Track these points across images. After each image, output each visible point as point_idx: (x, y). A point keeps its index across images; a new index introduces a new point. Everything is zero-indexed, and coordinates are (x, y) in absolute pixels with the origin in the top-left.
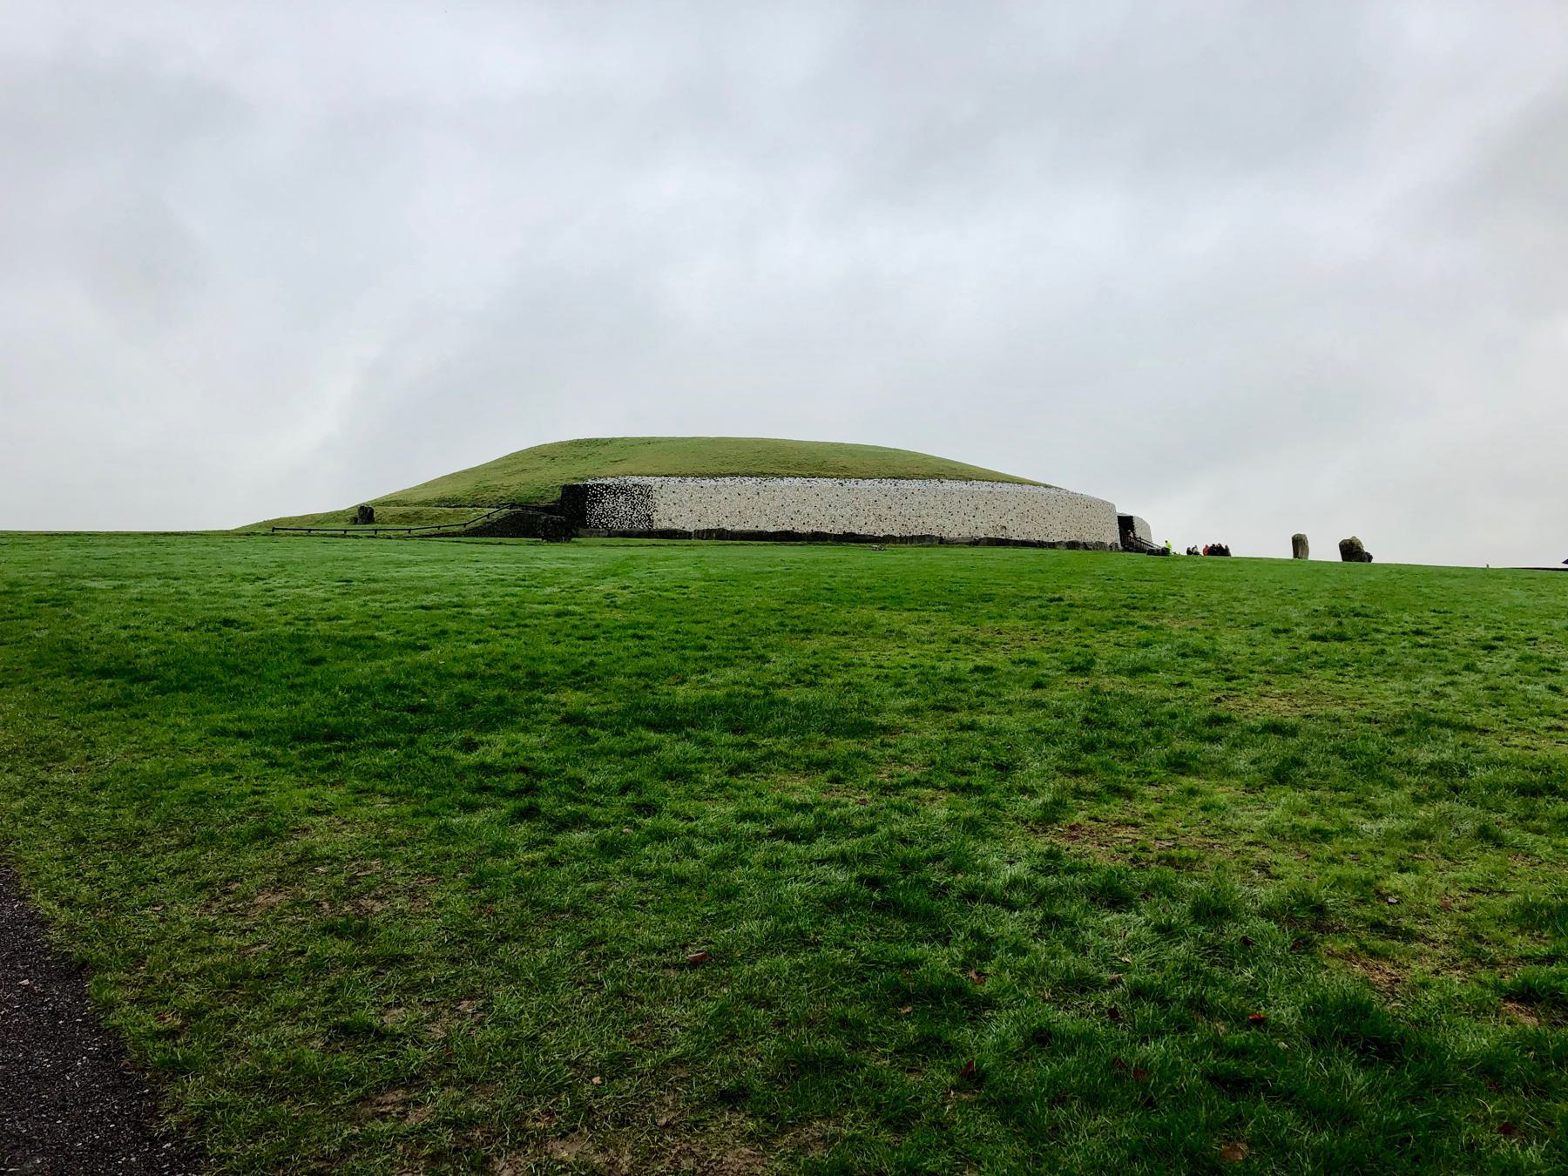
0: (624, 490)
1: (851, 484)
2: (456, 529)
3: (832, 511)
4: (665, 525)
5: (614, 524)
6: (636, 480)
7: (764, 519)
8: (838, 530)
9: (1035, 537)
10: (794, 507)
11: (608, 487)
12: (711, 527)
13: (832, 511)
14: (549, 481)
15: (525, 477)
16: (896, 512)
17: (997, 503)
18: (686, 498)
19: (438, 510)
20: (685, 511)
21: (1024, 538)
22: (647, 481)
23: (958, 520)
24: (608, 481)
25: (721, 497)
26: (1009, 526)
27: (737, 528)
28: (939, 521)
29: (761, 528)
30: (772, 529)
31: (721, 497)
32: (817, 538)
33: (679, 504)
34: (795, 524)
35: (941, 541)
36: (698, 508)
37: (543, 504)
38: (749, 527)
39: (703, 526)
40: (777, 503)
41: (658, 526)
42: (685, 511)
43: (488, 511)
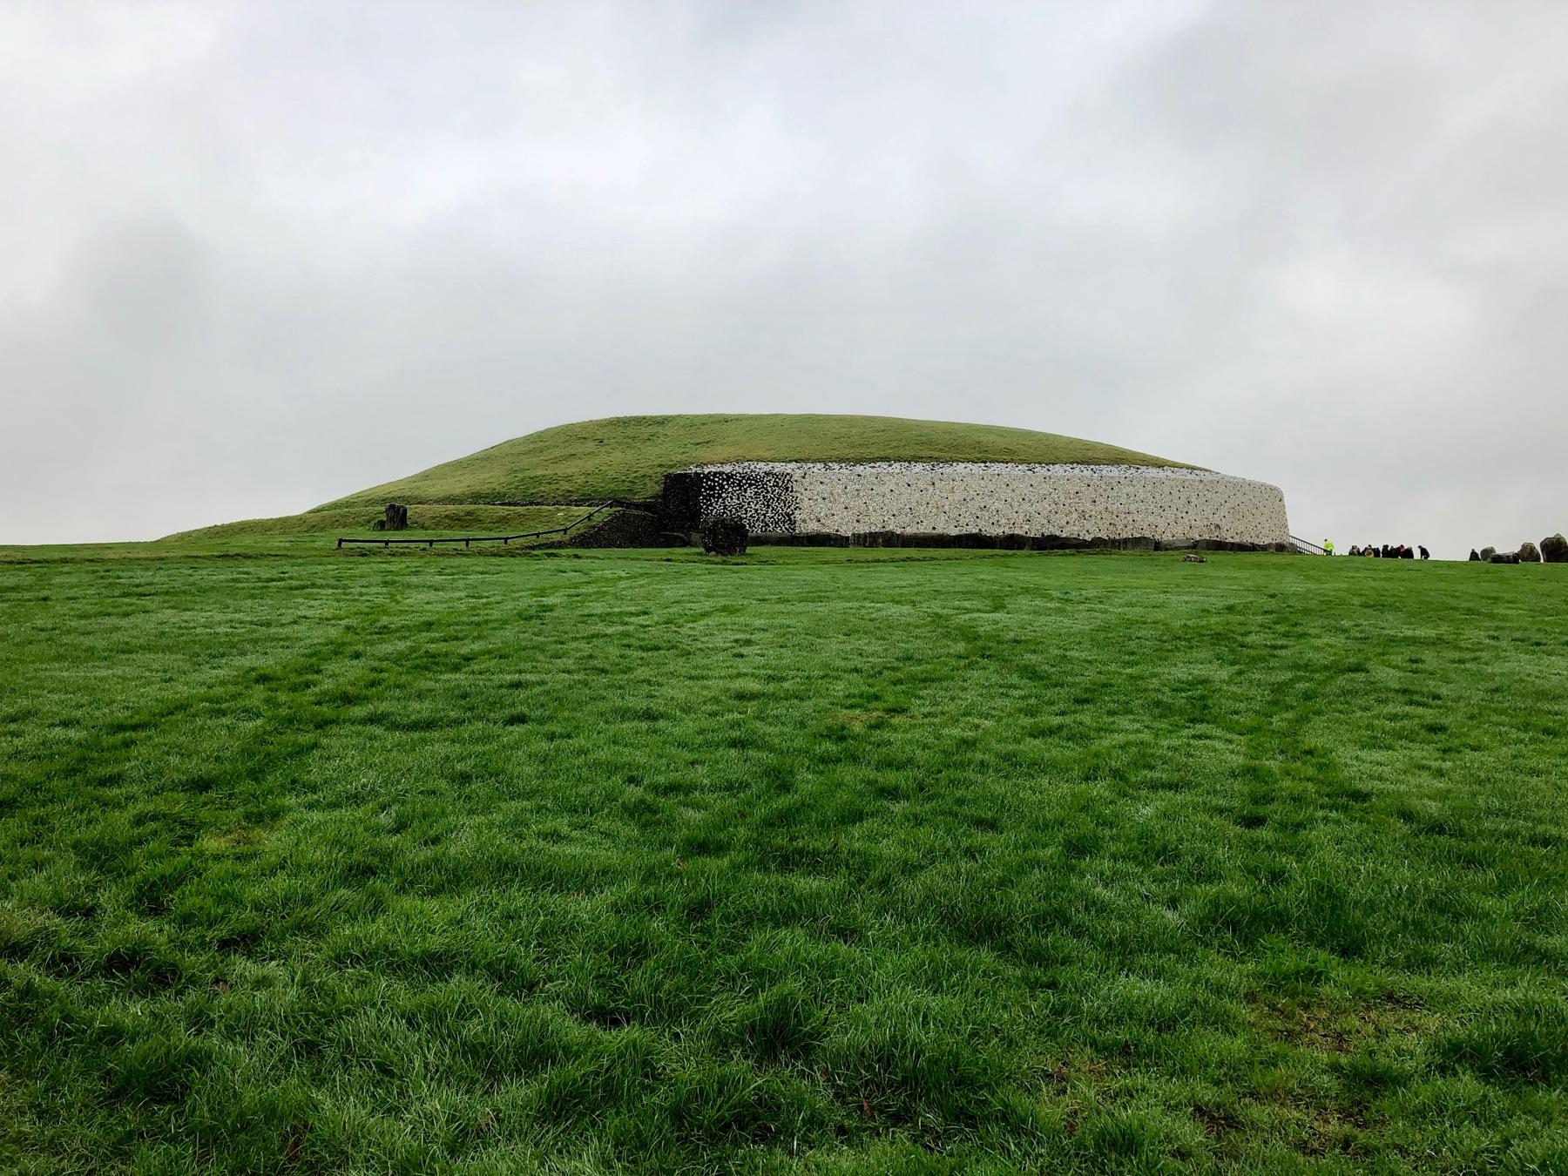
0: (751, 480)
2: (556, 537)
3: (1026, 506)
4: (812, 527)
7: (943, 518)
8: (1034, 530)
9: (1247, 540)
10: (979, 502)
11: (729, 477)
12: (874, 529)
13: (1026, 506)
14: (643, 468)
15: (590, 465)
16: (1101, 508)
17: (1209, 495)
18: (839, 489)
19: (501, 511)
20: (838, 508)
21: (1237, 540)
22: (779, 468)
23: (1171, 519)
24: (727, 469)
25: (885, 489)
26: (1223, 524)
27: (909, 531)
28: (1151, 519)
29: (939, 531)
30: (954, 532)
31: (885, 489)
32: (1013, 542)
33: (829, 500)
34: (981, 523)
35: (1158, 546)
36: (856, 505)
37: (637, 499)
38: (924, 529)
39: (863, 529)
40: (958, 496)
42: (838, 508)
43: (584, 511)
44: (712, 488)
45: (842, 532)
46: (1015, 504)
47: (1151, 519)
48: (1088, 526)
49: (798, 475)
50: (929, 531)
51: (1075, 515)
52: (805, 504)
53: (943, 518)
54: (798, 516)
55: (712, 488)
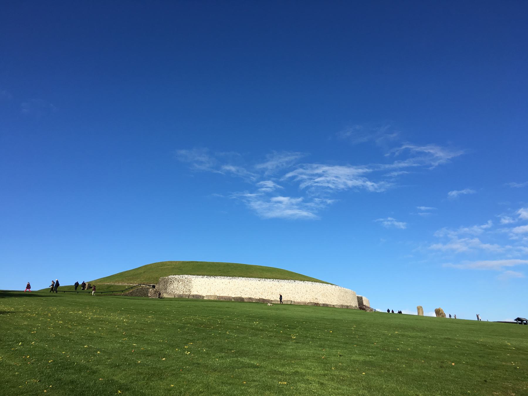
0: (182, 280)
1: (262, 280)
5: (177, 292)
6: (186, 276)
12: (212, 294)
13: (255, 290)
27: (221, 295)
28: (294, 295)
29: (230, 296)
30: (233, 296)
34: (242, 294)
39: (209, 294)
41: (192, 293)
45: (203, 295)
46: (252, 289)
47: (294, 295)
48: (274, 296)
49: (193, 279)
53: (231, 292)
54: (192, 290)
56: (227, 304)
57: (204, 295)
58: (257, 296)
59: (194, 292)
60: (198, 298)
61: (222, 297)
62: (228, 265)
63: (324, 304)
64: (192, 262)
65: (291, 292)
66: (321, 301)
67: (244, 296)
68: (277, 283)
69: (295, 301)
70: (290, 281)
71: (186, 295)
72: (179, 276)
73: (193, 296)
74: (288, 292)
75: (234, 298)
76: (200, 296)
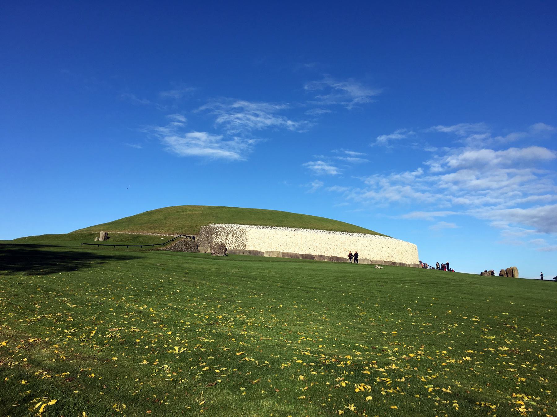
0: (233, 231)
13: (326, 245)
21: (399, 262)
27: (285, 251)
30: (301, 253)
39: (269, 250)
41: (248, 248)
44: (217, 233)
46: (323, 244)
49: (247, 230)
50: (293, 252)
51: (343, 250)
52: (249, 240)
54: (247, 244)
55: (217, 233)
56: (293, 265)
57: (263, 250)
58: (329, 253)
59: (250, 247)
60: (256, 256)
61: (287, 254)
62: (271, 212)
63: (400, 264)
64: (223, 207)
65: (366, 248)
66: (398, 260)
67: (313, 253)
68: (306, 233)
69: (372, 259)
70: (308, 230)
71: (240, 251)
72: (227, 225)
73: (250, 252)
74: (363, 248)
75: (302, 255)
76: (259, 252)
